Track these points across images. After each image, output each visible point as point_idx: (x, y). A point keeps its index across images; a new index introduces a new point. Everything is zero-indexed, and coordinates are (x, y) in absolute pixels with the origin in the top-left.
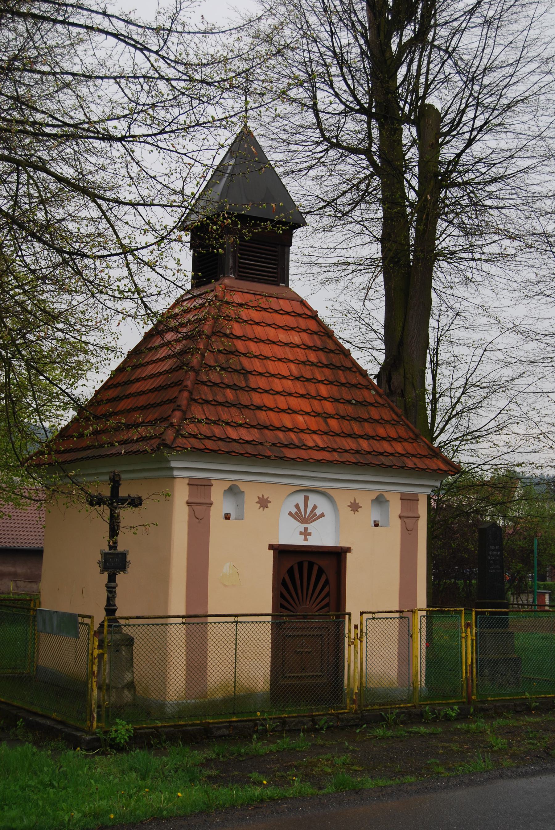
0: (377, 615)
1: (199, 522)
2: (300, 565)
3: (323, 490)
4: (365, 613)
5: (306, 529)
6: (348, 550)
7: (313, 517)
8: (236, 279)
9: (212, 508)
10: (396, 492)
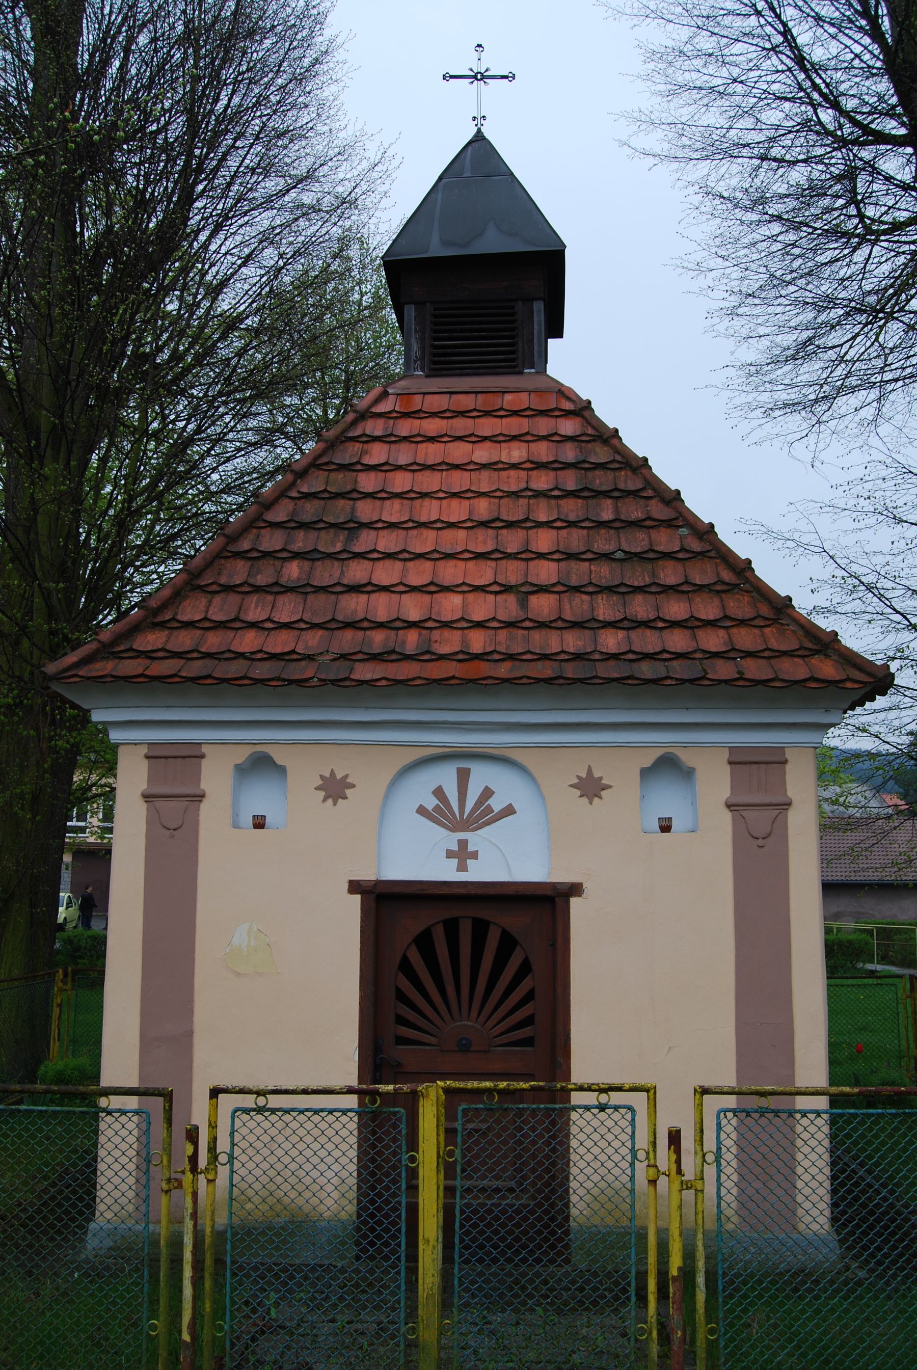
0: (275, 1101)
1: (172, 837)
2: (451, 927)
3: (495, 752)
4: (225, 1091)
5: (463, 844)
6: (575, 889)
7: (483, 815)
8: (427, 376)
9: (204, 806)
10: (714, 745)
